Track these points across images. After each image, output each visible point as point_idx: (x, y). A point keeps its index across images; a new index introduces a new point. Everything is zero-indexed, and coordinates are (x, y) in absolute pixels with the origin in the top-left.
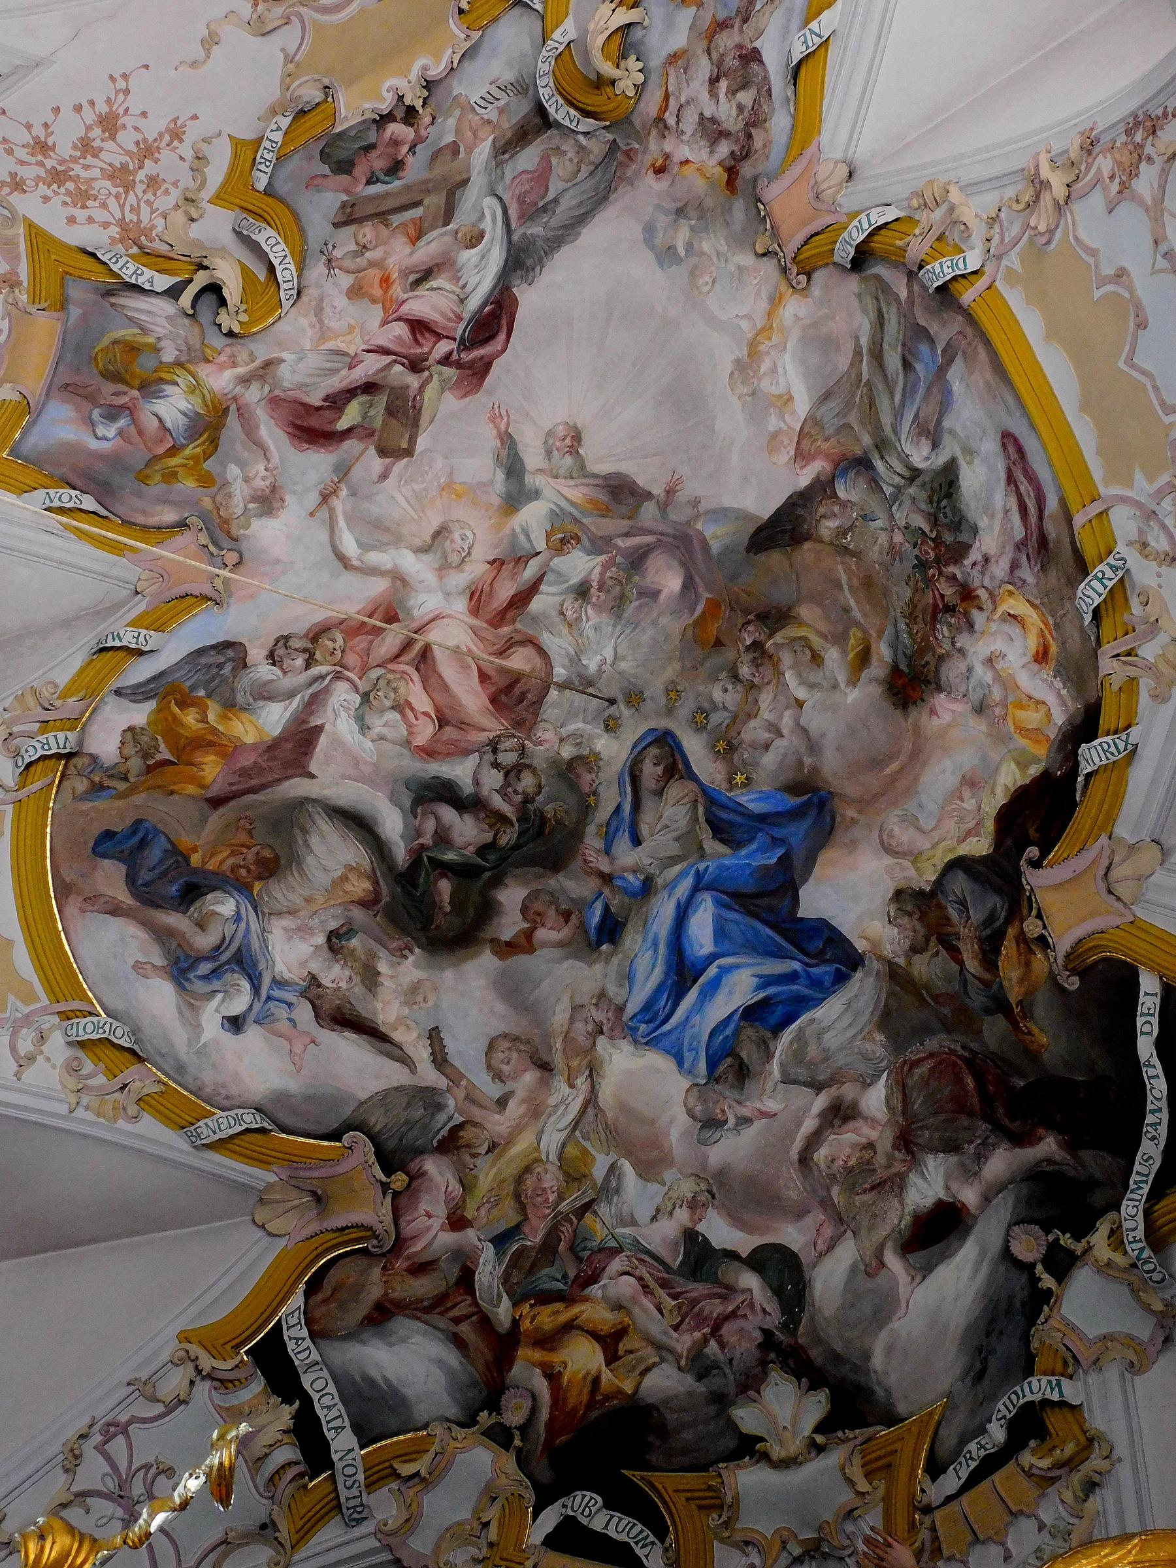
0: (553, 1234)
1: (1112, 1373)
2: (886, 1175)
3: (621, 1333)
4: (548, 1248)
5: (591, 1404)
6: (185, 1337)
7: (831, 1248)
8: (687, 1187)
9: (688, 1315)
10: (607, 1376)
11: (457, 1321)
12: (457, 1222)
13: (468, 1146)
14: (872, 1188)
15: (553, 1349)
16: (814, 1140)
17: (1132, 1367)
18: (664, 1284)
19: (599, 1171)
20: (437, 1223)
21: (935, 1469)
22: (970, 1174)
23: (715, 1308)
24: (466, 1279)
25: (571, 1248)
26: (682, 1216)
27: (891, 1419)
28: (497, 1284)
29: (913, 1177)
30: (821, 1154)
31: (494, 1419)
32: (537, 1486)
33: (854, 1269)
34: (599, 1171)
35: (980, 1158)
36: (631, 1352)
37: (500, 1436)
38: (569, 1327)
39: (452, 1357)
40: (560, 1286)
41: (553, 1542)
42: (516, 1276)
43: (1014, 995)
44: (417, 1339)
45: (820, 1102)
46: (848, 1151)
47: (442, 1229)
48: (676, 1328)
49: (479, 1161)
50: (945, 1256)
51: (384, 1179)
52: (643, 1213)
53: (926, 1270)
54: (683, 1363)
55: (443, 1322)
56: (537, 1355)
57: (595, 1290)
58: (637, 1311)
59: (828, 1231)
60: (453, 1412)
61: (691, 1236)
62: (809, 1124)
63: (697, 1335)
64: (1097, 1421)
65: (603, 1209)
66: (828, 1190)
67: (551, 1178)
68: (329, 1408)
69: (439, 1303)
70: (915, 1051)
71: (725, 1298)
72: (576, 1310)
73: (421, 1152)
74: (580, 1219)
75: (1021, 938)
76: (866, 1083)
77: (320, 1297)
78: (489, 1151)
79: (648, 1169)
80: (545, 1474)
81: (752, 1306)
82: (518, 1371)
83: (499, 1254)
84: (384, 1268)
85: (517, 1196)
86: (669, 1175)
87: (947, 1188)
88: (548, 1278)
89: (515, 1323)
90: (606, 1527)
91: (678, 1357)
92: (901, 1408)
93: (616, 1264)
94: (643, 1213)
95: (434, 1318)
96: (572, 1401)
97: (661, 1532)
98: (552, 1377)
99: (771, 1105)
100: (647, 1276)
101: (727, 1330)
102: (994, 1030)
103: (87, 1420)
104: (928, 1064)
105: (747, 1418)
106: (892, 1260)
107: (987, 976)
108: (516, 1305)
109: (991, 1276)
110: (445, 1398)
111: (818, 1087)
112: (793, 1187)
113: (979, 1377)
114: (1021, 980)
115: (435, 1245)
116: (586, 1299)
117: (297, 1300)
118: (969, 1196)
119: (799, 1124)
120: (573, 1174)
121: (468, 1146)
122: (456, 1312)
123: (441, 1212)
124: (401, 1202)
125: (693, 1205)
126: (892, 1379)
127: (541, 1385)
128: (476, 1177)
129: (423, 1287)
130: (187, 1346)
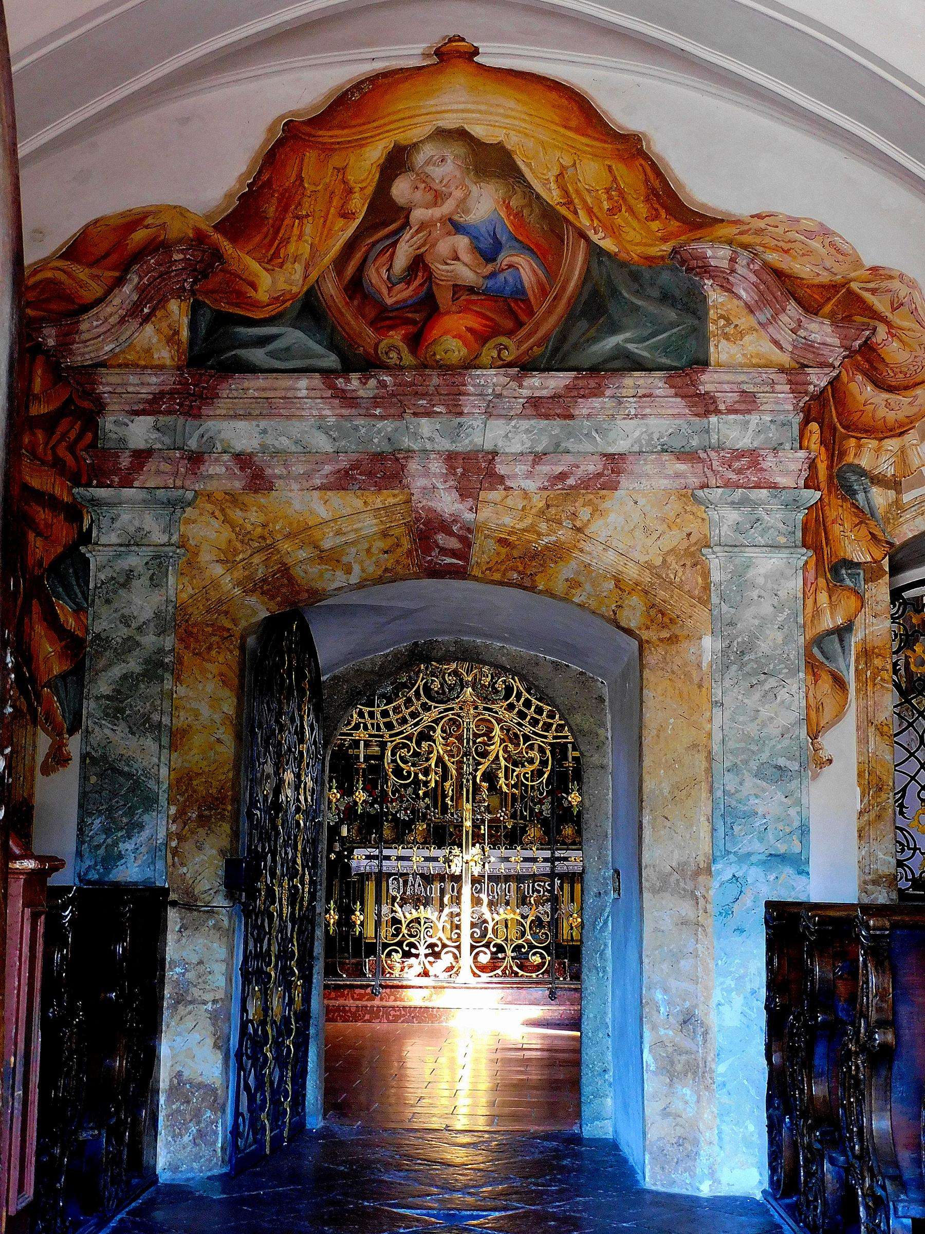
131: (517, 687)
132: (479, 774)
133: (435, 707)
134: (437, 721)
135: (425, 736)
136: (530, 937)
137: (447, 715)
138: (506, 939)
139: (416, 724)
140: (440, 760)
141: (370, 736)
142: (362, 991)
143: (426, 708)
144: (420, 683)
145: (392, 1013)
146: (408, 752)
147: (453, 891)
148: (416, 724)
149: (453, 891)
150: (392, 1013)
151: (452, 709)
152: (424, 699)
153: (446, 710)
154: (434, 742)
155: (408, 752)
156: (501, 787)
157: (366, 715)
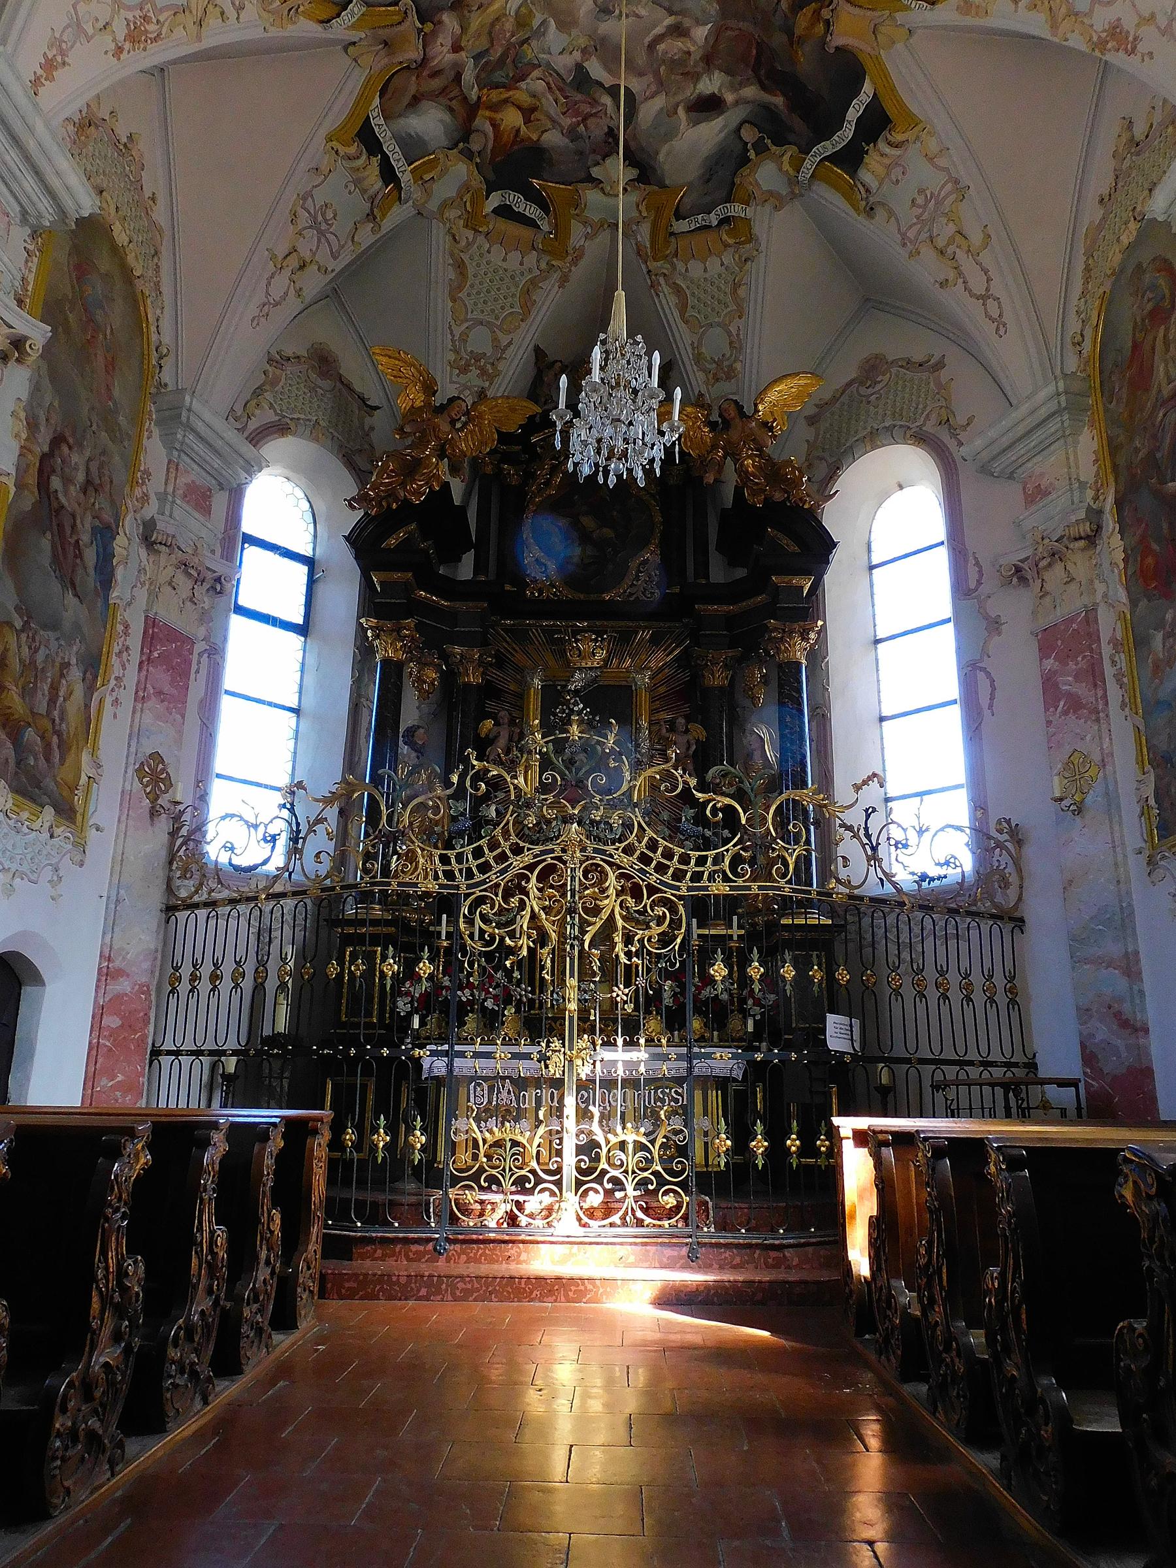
0: (505, 55)
1: (768, 207)
2: (692, 70)
3: (533, 109)
4: (501, 62)
5: (514, 143)
6: (329, 139)
7: (652, 97)
8: (583, 41)
9: (570, 108)
10: (523, 128)
11: (451, 100)
12: (456, 48)
13: (468, 6)
14: (682, 74)
15: (496, 111)
16: (659, 39)
17: (776, 208)
18: (561, 90)
19: (535, 23)
20: (445, 49)
21: (679, 216)
22: (734, 88)
23: (586, 109)
24: (458, 77)
25: (514, 62)
26: (577, 55)
27: (663, 186)
28: (473, 80)
29: (705, 78)
30: (661, 47)
31: (466, 145)
32: (487, 182)
33: (662, 109)
34: (535, 23)
35: (742, 85)
36: (538, 120)
37: (469, 155)
38: (506, 101)
39: (447, 117)
40: (504, 80)
41: (496, 211)
42: (483, 75)
43: (798, 32)
44: (433, 111)
45: (669, 21)
46: (676, 51)
47: (448, 52)
48: (564, 114)
49: (472, 15)
50: (707, 120)
51: (421, 26)
52: (556, 49)
53: (696, 123)
54: (565, 131)
55: (445, 101)
56: (487, 113)
57: (523, 85)
58: (543, 100)
59: (653, 88)
60: (445, 143)
61: (579, 67)
62: (659, 30)
63: (574, 120)
64: (756, 230)
65: (534, 43)
66: (660, 65)
67: (509, 25)
68: (398, 160)
69: (443, 91)
70: (732, 23)
71: (592, 106)
72: (511, 93)
73: (441, 9)
74: (520, 47)
75: (817, 13)
76: (699, 22)
77: (387, 96)
78: (479, 8)
79: (563, 26)
80: (491, 176)
81: (606, 114)
82: (477, 122)
83: (476, 66)
84: (418, 77)
85: (490, 33)
86: (574, 32)
87: (720, 90)
88: (499, 76)
89: (479, 98)
90: (525, 210)
91: (562, 128)
92: (667, 182)
93: (536, 73)
94: (556, 49)
95: (440, 99)
96: (505, 138)
97: (547, 212)
98: (495, 126)
99: (643, 12)
100: (551, 82)
101: (591, 122)
102: (778, 40)
103: (295, 196)
104: (737, 33)
105: (595, 172)
106: (681, 112)
107: (789, 15)
108: (480, 90)
109: (726, 137)
110: (443, 138)
111: (671, 12)
112: (641, 59)
113: (708, 181)
114: (807, 28)
115: (446, 59)
116: (517, 88)
117: (377, 101)
118: (729, 97)
119: (655, 26)
120: (522, 22)
121: (468, 6)
122: (452, 95)
123: (448, 42)
124: (427, 40)
125: (584, 51)
126: (666, 167)
127: (489, 129)
128: (469, 24)
129: (436, 83)
130: (330, 144)
131: (639, 824)
132: (587, 938)
133: (529, 849)
135: (517, 887)
136: (659, 1168)
137: (544, 860)
138: (626, 1172)
141: (441, 886)
142: (422, 1248)
145: (461, 1285)
146: (492, 908)
147: (552, 1101)
149: (552, 1101)
150: (461, 1285)
151: (552, 851)
153: (543, 853)
154: (527, 895)
155: (492, 908)
156: (617, 956)
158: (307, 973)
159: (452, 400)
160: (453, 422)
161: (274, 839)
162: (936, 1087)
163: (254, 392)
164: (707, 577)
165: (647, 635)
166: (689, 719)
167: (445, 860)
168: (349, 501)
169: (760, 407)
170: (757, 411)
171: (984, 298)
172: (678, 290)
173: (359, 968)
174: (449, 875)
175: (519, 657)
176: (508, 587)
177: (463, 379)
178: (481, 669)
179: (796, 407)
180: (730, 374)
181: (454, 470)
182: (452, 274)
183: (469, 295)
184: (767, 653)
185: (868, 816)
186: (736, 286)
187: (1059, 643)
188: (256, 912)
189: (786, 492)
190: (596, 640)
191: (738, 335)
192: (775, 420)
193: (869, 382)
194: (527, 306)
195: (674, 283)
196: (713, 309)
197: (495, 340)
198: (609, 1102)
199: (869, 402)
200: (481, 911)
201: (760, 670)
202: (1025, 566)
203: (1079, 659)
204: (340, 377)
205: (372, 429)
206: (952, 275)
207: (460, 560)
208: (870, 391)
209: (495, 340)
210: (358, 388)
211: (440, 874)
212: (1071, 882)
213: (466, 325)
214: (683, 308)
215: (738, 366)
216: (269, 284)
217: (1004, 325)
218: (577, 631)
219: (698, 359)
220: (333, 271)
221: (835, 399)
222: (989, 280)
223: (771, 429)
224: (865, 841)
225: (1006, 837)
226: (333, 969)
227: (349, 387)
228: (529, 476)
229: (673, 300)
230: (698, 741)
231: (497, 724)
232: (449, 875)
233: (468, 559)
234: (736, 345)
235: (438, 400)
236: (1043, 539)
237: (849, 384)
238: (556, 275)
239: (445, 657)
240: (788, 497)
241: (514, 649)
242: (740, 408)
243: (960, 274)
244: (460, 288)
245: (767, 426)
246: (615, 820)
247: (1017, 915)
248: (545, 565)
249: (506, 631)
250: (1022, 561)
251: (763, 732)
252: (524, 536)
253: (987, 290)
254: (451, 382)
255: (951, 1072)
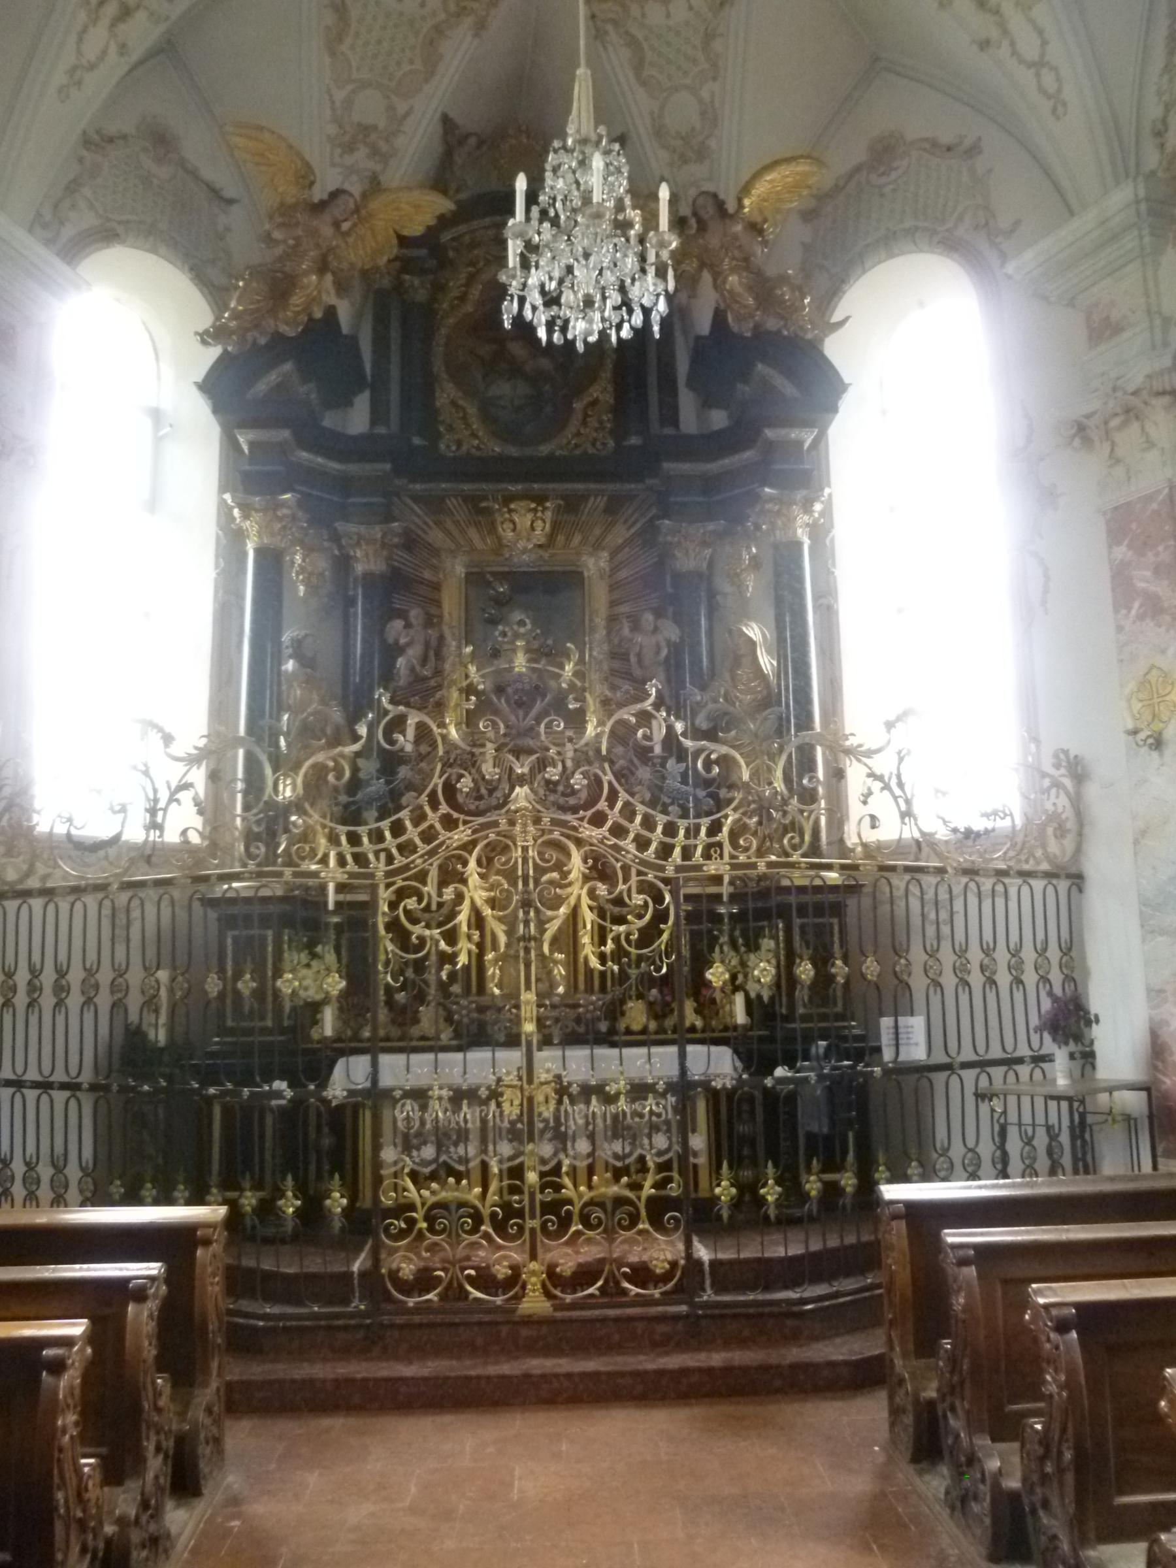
132: (548, 936)
134: (469, 846)
135: (451, 875)
137: (487, 837)
139: (432, 853)
140: (478, 921)
141: (352, 875)
143: (450, 823)
144: (437, 781)
146: (420, 901)
148: (432, 853)
150: (403, 1389)
152: (444, 808)
154: (464, 881)
156: (586, 959)
157: (343, 839)
158: (181, 989)
159: (335, 194)
160: (337, 225)
161: (123, 810)
162: (980, 1096)
163: (67, 188)
164: (675, 423)
165: (601, 502)
166: (659, 613)
167: (354, 839)
168: (201, 335)
169: (747, 202)
170: (741, 206)
171: (1038, 65)
172: (633, 43)
173: (247, 985)
174: (360, 859)
175: (436, 537)
176: (417, 441)
177: (349, 160)
178: (385, 553)
179: (791, 202)
180: (702, 154)
181: (341, 288)
182: (329, 19)
183: (352, 47)
184: (758, 527)
185: (901, 760)
186: (709, 37)
187: (1134, 526)
188: (107, 903)
189: (782, 317)
190: (535, 510)
191: (712, 102)
192: (765, 221)
193: (882, 169)
194: (431, 64)
195: (627, 33)
196: (679, 68)
197: (391, 108)
198: (574, 1119)
199: (882, 195)
200: (405, 908)
201: (749, 548)
202: (1091, 423)
203: (1161, 548)
204: (182, 163)
205: (228, 229)
206: (994, 33)
207: (350, 404)
208: (884, 180)
209: (391, 108)
210: (207, 173)
211: (349, 858)
212: (1144, 833)
213: (350, 87)
214: (639, 66)
215: (712, 143)
216: (80, 40)
217: (1064, 104)
218: (508, 499)
219: (659, 132)
220: (167, 18)
221: (837, 189)
222: (1044, 43)
223: (761, 232)
224: (898, 792)
225: (1063, 771)
226: (213, 986)
227: (194, 174)
228: (439, 288)
229: (625, 53)
230: (669, 643)
231: (408, 625)
232: (360, 859)
233: (362, 402)
234: (710, 115)
235: (318, 194)
236: (1115, 389)
237: (858, 169)
238: (468, 21)
239: (336, 538)
240: (785, 326)
241: (425, 523)
242: (720, 205)
243: (1005, 31)
244: (340, 39)
245: (755, 228)
246: (578, 781)
247: (1073, 870)
248: (464, 409)
249: (416, 499)
250: (1088, 416)
251: (754, 632)
252: (435, 370)
253: (1042, 55)
254: (333, 165)
255: (997, 1072)
